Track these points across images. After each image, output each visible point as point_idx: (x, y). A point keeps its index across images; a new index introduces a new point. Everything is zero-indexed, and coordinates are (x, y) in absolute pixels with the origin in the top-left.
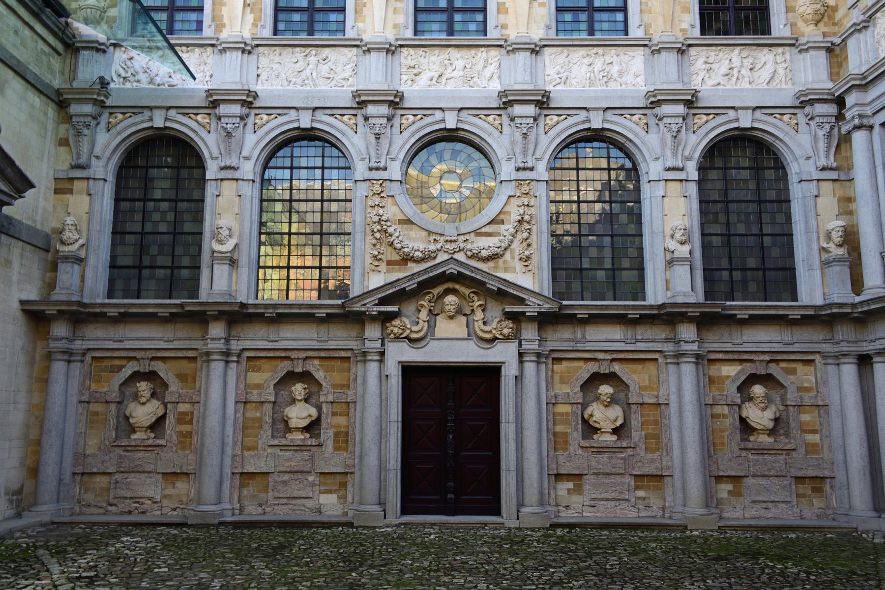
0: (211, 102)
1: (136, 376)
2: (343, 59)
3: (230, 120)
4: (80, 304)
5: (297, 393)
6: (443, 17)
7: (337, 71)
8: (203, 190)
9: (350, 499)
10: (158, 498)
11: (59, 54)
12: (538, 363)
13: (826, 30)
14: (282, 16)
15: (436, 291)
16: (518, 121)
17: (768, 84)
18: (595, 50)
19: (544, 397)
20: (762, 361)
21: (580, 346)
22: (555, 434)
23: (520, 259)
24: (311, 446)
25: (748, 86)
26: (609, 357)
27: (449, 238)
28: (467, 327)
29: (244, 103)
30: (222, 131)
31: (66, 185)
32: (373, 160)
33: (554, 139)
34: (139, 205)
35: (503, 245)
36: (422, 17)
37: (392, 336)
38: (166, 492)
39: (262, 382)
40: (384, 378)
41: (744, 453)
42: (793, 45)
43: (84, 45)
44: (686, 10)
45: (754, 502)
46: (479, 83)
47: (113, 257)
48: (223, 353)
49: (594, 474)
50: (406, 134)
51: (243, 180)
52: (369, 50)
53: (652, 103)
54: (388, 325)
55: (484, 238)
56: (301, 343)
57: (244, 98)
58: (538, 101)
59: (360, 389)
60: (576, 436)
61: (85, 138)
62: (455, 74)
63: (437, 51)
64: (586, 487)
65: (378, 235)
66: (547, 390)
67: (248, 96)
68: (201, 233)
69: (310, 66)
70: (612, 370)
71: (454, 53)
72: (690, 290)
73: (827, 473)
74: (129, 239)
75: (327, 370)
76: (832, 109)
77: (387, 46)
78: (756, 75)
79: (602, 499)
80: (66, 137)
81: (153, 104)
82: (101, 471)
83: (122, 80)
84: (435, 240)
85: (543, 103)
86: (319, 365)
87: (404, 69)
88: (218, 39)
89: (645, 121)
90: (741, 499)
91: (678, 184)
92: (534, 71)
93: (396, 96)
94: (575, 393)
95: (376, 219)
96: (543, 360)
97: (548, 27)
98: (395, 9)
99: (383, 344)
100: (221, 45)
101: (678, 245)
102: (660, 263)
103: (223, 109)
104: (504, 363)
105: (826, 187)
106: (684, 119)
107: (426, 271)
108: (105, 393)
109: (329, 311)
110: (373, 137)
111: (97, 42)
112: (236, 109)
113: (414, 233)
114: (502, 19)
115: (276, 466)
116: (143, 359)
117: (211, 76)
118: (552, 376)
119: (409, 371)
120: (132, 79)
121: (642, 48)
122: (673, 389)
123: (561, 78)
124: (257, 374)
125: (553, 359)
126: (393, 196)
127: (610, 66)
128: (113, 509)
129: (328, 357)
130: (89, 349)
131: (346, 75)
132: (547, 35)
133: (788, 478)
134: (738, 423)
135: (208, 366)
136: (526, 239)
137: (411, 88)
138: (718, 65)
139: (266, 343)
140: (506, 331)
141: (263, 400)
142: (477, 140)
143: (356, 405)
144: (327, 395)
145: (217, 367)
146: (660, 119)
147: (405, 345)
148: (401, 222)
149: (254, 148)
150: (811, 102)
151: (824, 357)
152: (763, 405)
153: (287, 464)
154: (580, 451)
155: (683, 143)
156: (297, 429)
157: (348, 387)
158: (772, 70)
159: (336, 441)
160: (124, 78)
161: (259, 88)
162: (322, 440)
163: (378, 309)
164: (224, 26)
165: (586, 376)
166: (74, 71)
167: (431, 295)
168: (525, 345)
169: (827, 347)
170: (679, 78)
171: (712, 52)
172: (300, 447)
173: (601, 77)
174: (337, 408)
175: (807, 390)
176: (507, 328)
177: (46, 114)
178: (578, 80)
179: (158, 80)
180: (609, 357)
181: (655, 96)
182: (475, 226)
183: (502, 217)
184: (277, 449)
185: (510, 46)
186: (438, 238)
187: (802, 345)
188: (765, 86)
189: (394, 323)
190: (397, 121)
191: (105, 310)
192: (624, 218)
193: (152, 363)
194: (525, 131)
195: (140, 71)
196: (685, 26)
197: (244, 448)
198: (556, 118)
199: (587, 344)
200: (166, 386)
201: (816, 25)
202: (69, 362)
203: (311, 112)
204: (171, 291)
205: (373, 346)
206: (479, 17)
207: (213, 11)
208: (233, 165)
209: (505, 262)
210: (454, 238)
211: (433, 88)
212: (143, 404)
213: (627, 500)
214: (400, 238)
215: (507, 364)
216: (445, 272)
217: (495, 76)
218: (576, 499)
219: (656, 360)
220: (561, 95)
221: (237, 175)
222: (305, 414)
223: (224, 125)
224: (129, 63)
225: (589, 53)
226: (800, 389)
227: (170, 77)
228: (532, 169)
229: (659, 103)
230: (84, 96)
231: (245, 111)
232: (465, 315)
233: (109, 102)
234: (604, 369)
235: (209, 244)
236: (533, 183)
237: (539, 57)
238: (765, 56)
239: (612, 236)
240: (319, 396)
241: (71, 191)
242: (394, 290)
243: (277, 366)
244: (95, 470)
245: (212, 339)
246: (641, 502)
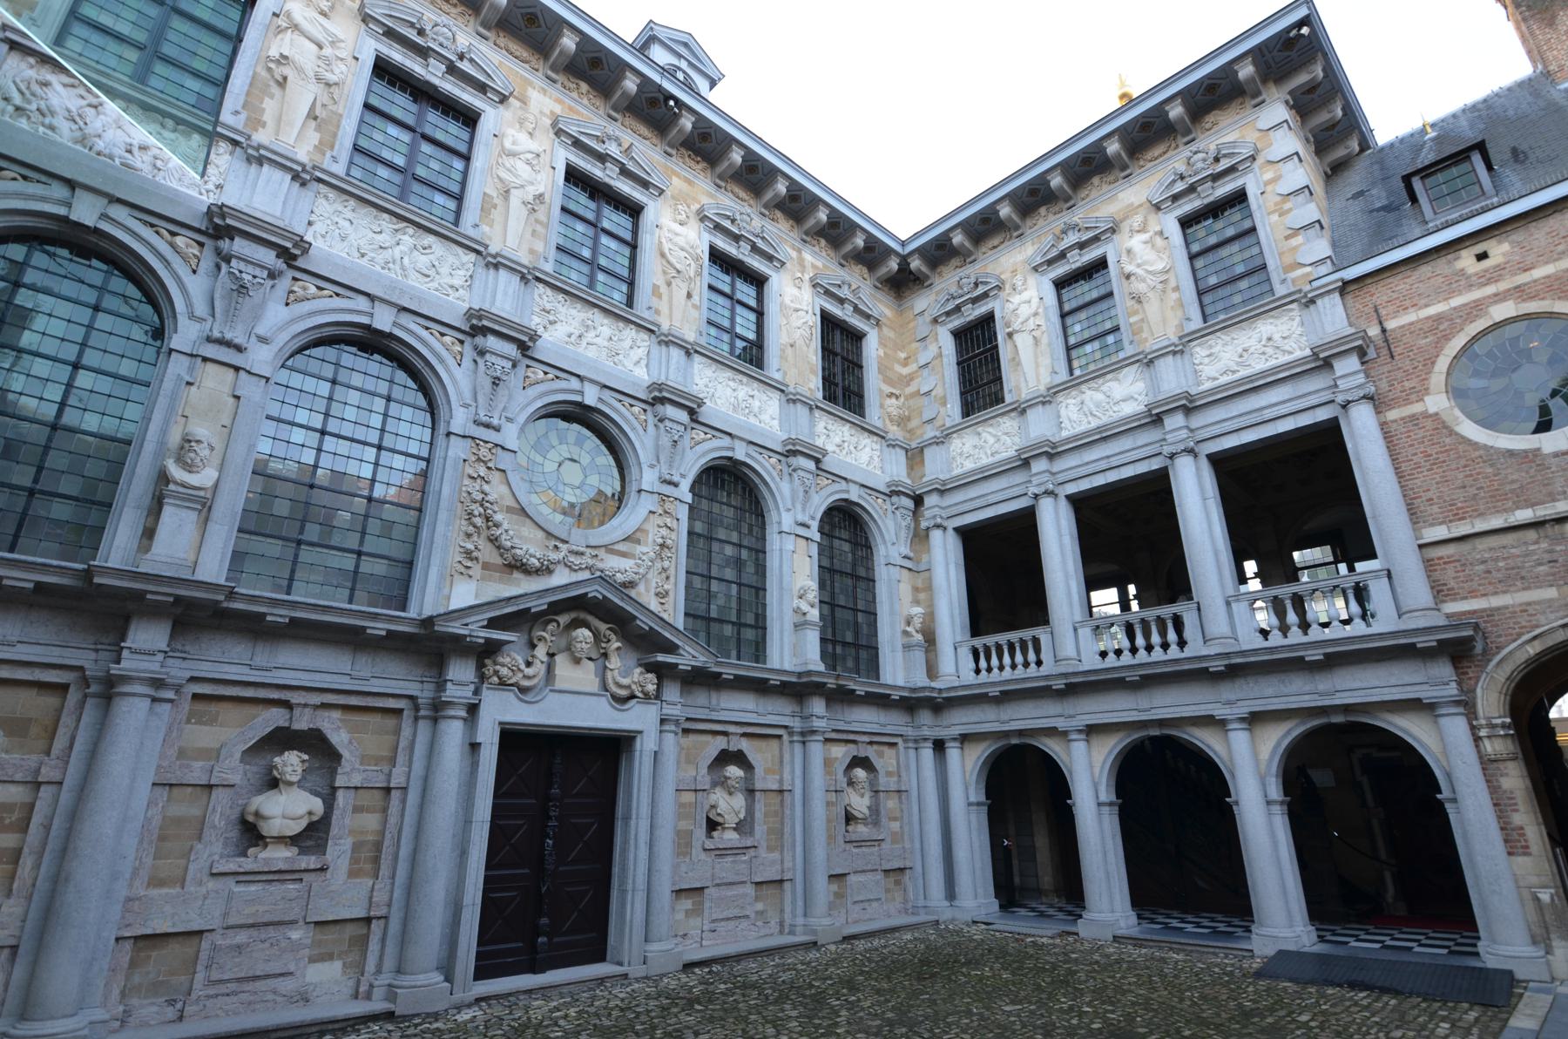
3: (250, 269)
7: (440, 270)
15: (564, 619)
16: (667, 423)
18: (740, 377)
21: (714, 716)
23: (657, 595)
27: (574, 548)
35: (641, 571)
41: (848, 846)
50: (532, 392)
51: (249, 372)
54: (488, 661)
55: (616, 558)
56: (318, 676)
57: (289, 245)
67: (296, 245)
69: (401, 247)
70: (740, 747)
79: (723, 920)
81: (81, 179)
84: (556, 547)
86: (341, 720)
88: (249, 138)
95: (479, 497)
98: (534, 231)
99: (477, 692)
102: (788, 626)
104: (641, 732)
115: (225, 915)
122: (798, 772)
124: (206, 728)
126: (504, 471)
129: (357, 706)
131: (457, 282)
139: (246, 670)
143: (406, 795)
147: (510, 697)
151: (905, 741)
154: (703, 856)
156: (281, 839)
159: (354, 860)
161: (318, 244)
162: (328, 856)
163: (488, 635)
165: (715, 754)
168: (669, 710)
169: (909, 732)
174: (367, 798)
179: (100, 145)
181: (794, 445)
182: (606, 540)
183: (638, 535)
184: (231, 881)
186: (560, 545)
189: (500, 659)
194: (676, 438)
195: (62, 113)
197: (156, 882)
204: (16, 536)
205: (459, 694)
208: (237, 341)
215: (645, 734)
217: (644, 363)
218: (695, 922)
219: (779, 737)
222: (302, 810)
224: (36, 88)
227: (129, 151)
231: (280, 264)
239: (740, 585)
245: (133, 651)
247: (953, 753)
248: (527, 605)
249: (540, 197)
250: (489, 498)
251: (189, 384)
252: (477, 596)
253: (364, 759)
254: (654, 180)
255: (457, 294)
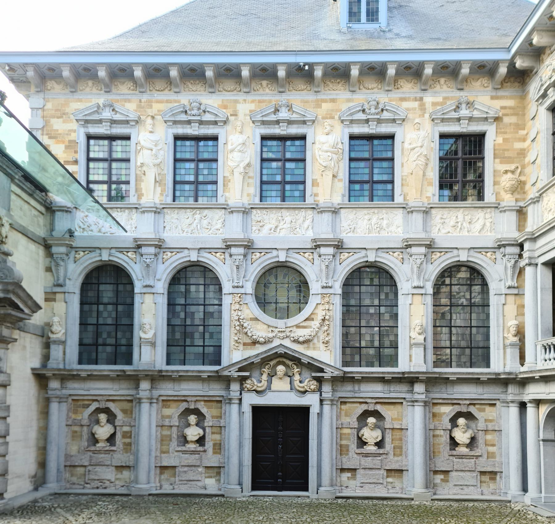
0: (137, 245)
1: (98, 411)
2: (217, 217)
4: (64, 370)
5: (191, 421)
6: (278, 187)
8: (133, 298)
9: (222, 481)
10: (113, 480)
11: (43, 214)
12: (332, 405)
13: (518, 196)
14: (178, 187)
15: (272, 363)
16: (322, 257)
17: (479, 232)
18: (373, 210)
19: (335, 424)
20: (465, 404)
22: (341, 446)
23: (323, 342)
24: (200, 451)
25: (467, 234)
26: (374, 401)
27: (280, 330)
28: (290, 384)
29: (156, 246)
30: (144, 264)
31: (51, 296)
32: (236, 281)
33: (345, 268)
34: (95, 307)
36: (265, 187)
37: (246, 389)
38: (118, 476)
39: (170, 414)
40: (241, 414)
41: (451, 458)
42: (497, 207)
43: (58, 209)
44: (430, 184)
45: (455, 485)
46: (300, 232)
47: (81, 339)
48: (148, 399)
49: (363, 468)
52: (232, 212)
53: (406, 245)
54: (244, 382)
55: (301, 330)
57: (157, 243)
58: (336, 245)
59: (227, 419)
60: (353, 446)
61: (62, 268)
62: (285, 226)
63: (274, 211)
64: (358, 476)
65: (238, 328)
66: (337, 420)
68: (133, 325)
69: (196, 221)
70: (376, 409)
71: (285, 212)
72: (423, 362)
73: (497, 469)
74: (90, 328)
75: (208, 408)
76: (517, 250)
77: (243, 209)
78: (472, 226)
79: (367, 483)
80: (49, 266)
82: (80, 464)
83: (81, 230)
84: (272, 330)
85: (339, 246)
87: (254, 223)
89: (401, 257)
90: (448, 483)
91: (420, 297)
92: (334, 225)
93: (248, 242)
94: (354, 422)
95: (237, 318)
96: (335, 403)
97: (343, 196)
98: (248, 183)
99: (241, 394)
100: (141, 208)
101: (417, 335)
103: (144, 250)
105: (511, 299)
106: (425, 256)
107: (266, 352)
108: (80, 420)
109: (209, 374)
110: (235, 267)
111: (65, 207)
112: (152, 250)
113: (260, 326)
114: (315, 190)
115: (180, 462)
116: (101, 401)
117: (136, 228)
118: (340, 412)
119: (257, 410)
120: (87, 229)
121: (402, 209)
123: (350, 229)
125: (341, 402)
127: (381, 220)
128: (88, 486)
129: (209, 400)
130: (70, 395)
132: (343, 201)
133: (476, 472)
134: (448, 440)
135: (140, 406)
136: (327, 331)
137: (258, 235)
138: (449, 220)
140: (312, 387)
141: (172, 425)
142: (298, 268)
144: (208, 423)
145: (145, 406)
146: (411, 256)
147: (254, 394)
148: (251, 319)
149: (163, 273)
150: (504, 246)
152: (463, 430)
153: (186, 461)
154: (355, 456)
155: (424, 271)
156: (192, 442)
157: (221, 417)
158: (482, 223)
159: (214, 449)
160: (83, 229)
162: (206, 448)
164: (142, 195)
166: (53, 224)
167: (269, 365)
170: (423, 228)
171: (445, 212)
172: (193, 452)
173: (375, 228)
174: (215, 430)
175: (491, 421)
176: (314, 385)
177: (38, 254)
178: (361, 230)
179: (103, 230)
180: (374, 401)
181: (407, 242)
183: (312, 316)
184: (180, 454)
185: (319, 209)
186: (274, 329)
187: (489, 395)
188: (477, 234)
189: (247, 382)
190: (249, 257)
191: (79, 373)
192: (387, 316)
193: (107, 403)
194: (327, 264)
195: (92, 223)
196: (429, 194)
197: (163, 452)
198: (347, 255)
199: (361, 394)
200: (115, 416)
201: (512, 194)
202: (59, 402)
203: (197, 251)
205: (235, 395)
206: (301, 187)
207: (136, 185)
209: (314, 344)
210: (284, 330)
211: (272, 235)
212: (102, 426)
213: (382, 484)
214: (251, 330)
216: (277, 352)
217: (310, 228)
219: (402, 403)
220: (350, 242)
221: (153, 290)
222: (196, 433)
223: (145, 260)
225: (369, 212)
226: (486, 421)
228: (331, 287)
229: (409, 246)
230: (60, 242)
231: (158, 250)
232: (289, 376)
233: (74, 245)
234: (371, 408)
235: (138, 333)
236: (332, 296)
237: (337, 215)
238: (480, 215)
240: (204, 422)
241: (54, 300)
242: (247, 363)
243: (180, 405)
244: (77, 464)
246: (390, 485)
247: (530, 410)
248: (252, 361)
249: (249, 165)
250: (241, 317)
251: (142, 303)
252: (242, 356)
253: (213, 417)
254: (309, 117)
255: (220, 232)
